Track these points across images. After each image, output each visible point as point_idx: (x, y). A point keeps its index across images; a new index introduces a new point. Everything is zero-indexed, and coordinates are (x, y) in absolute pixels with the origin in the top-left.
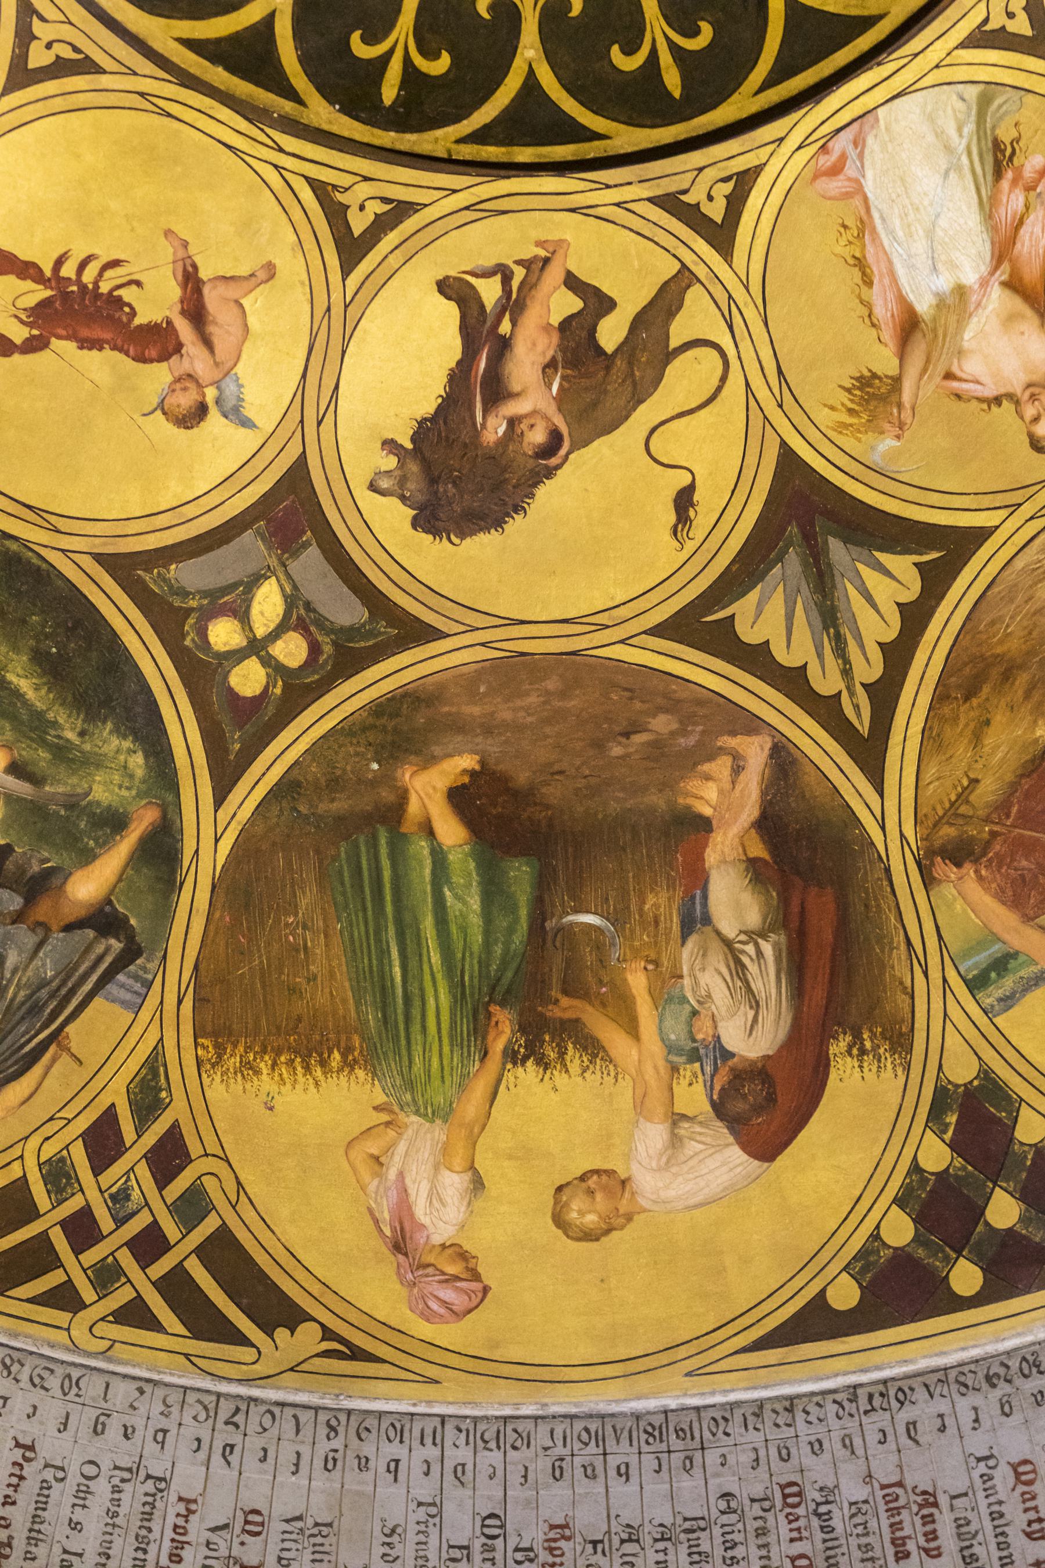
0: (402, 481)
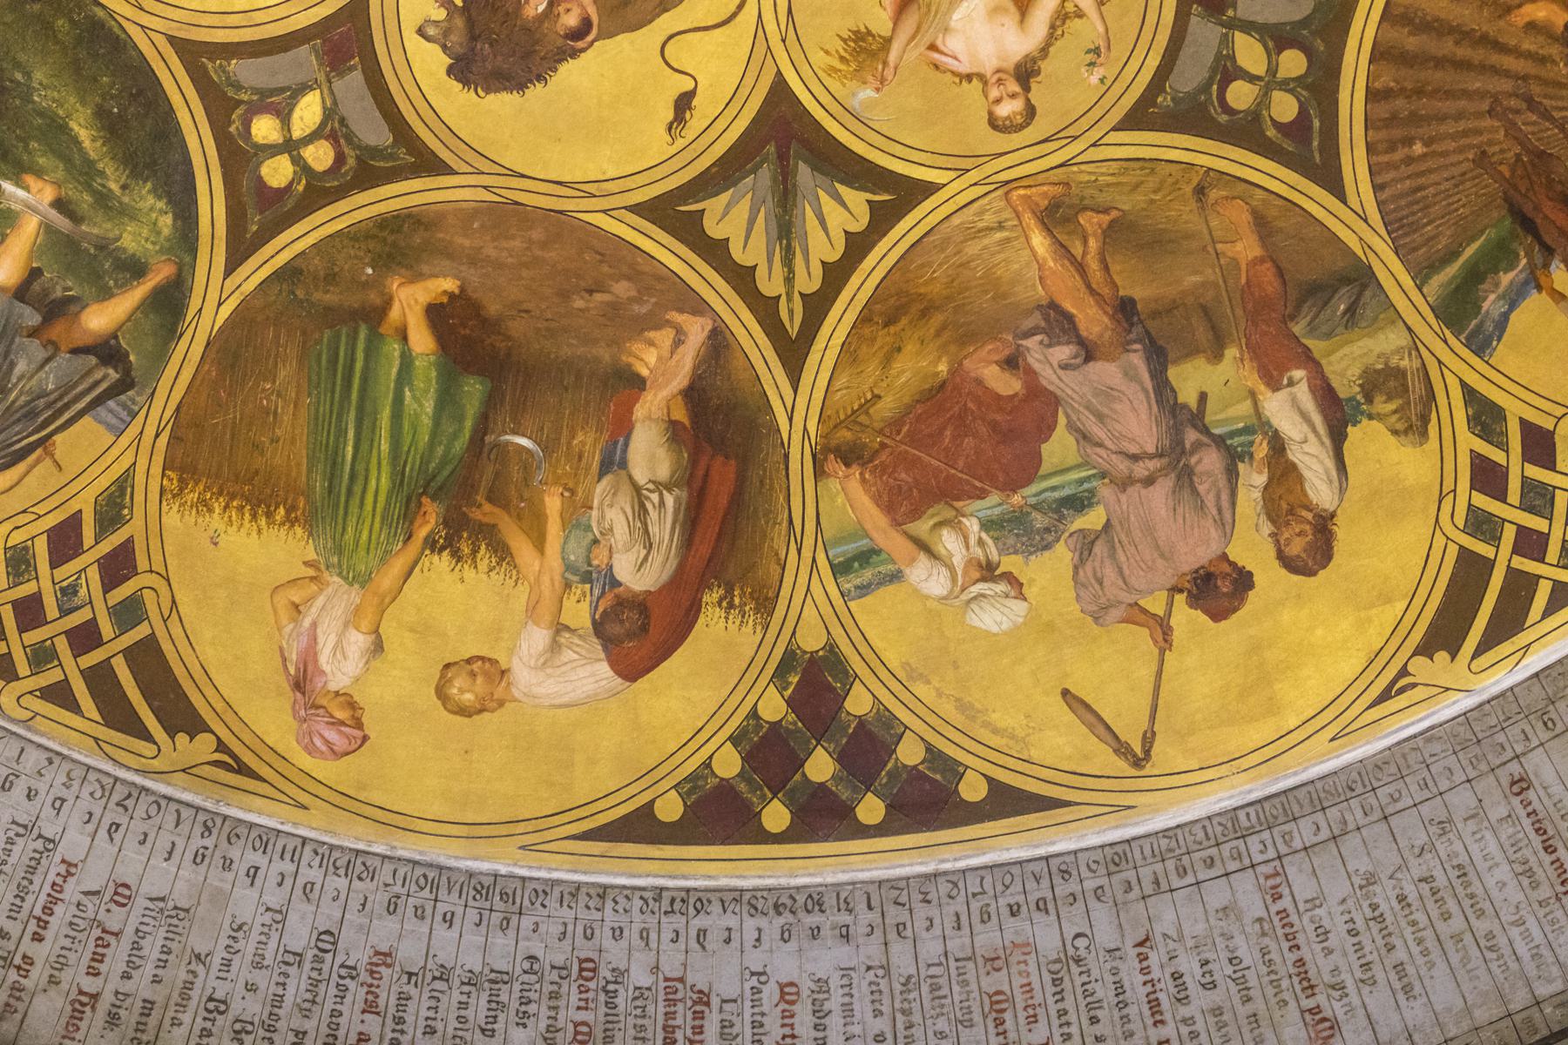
0: (446, 33)
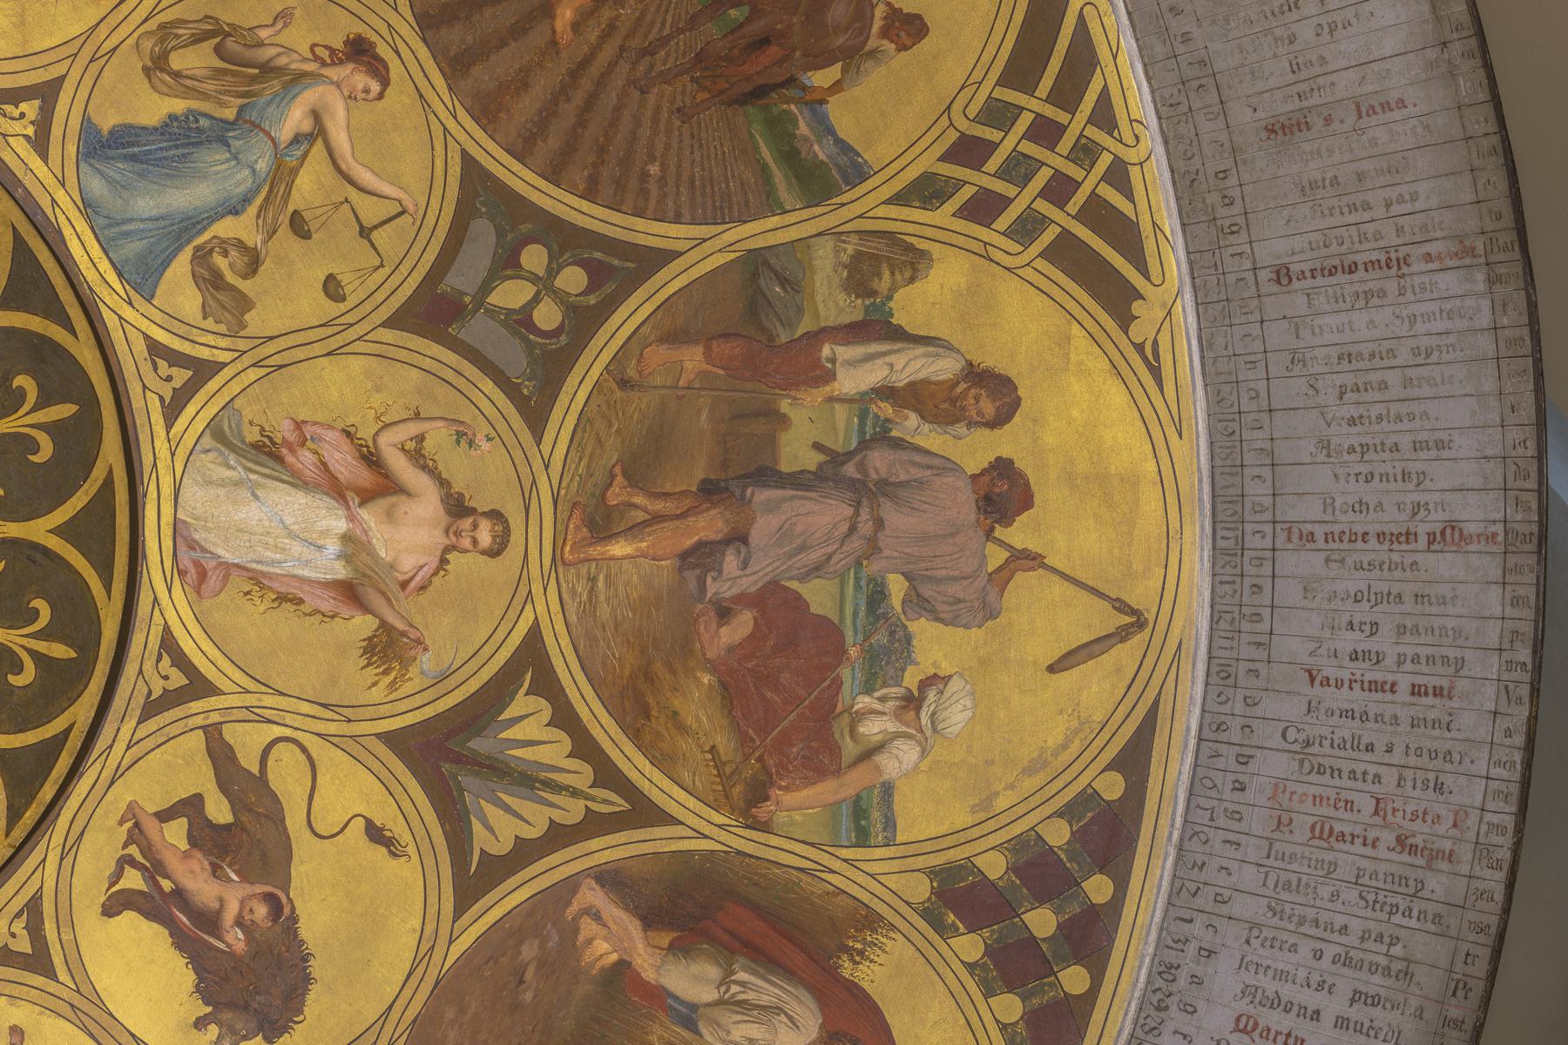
0: (234, 1032)
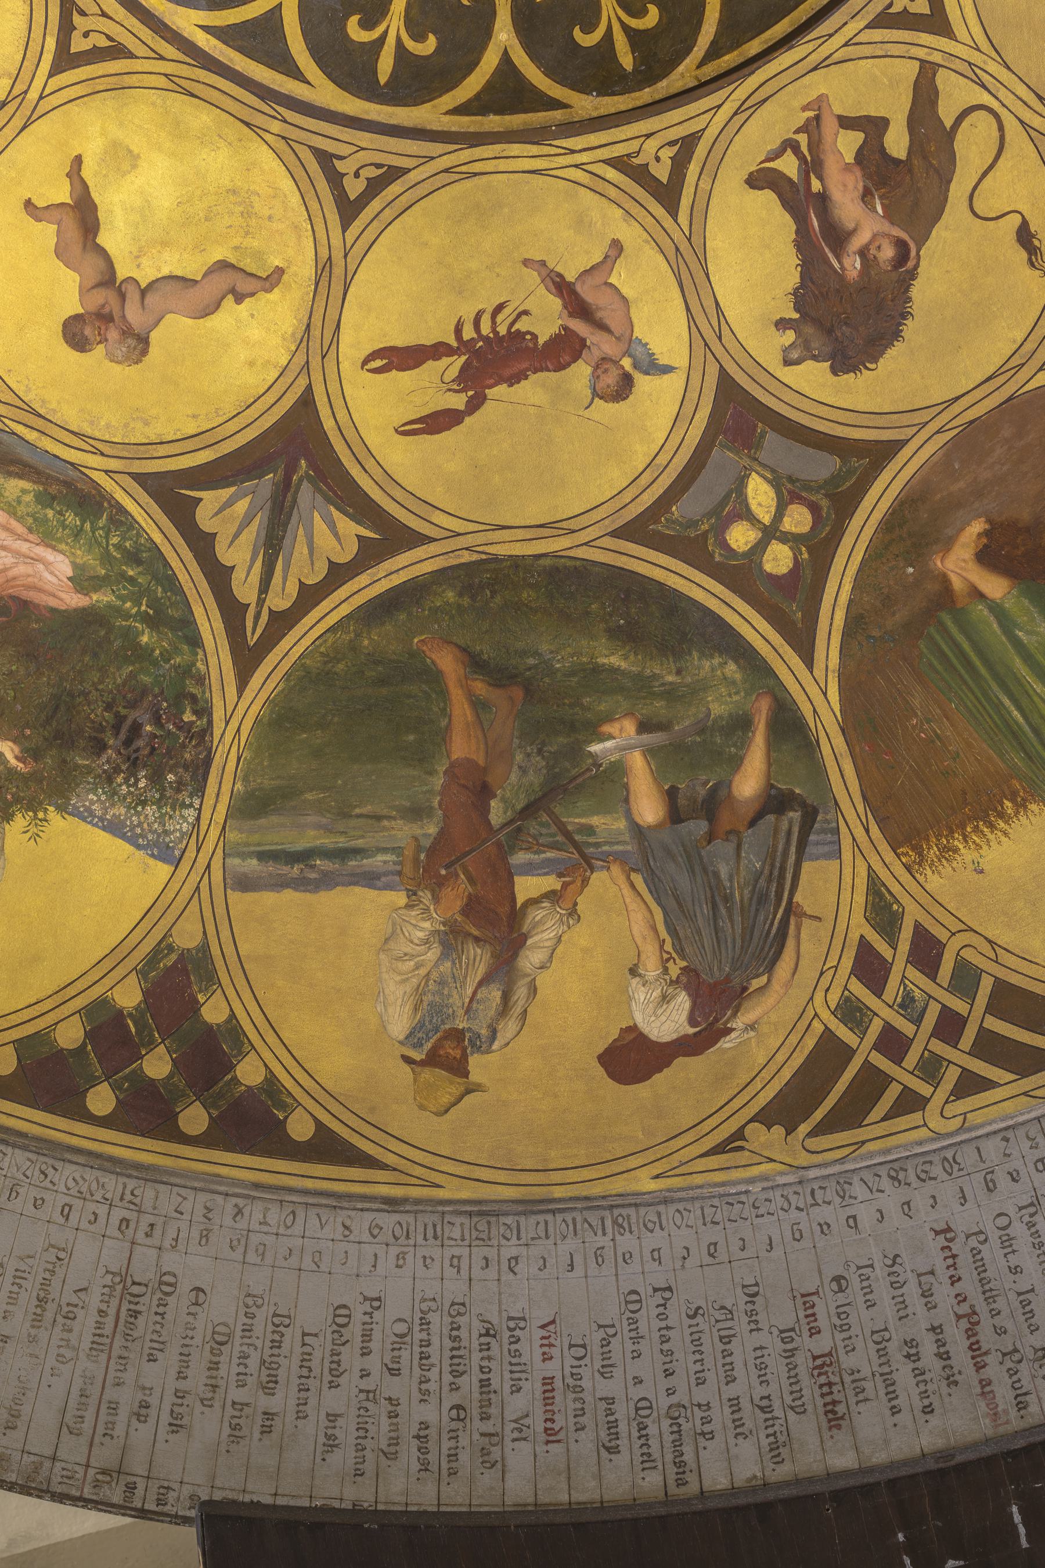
0: (807, 345)
